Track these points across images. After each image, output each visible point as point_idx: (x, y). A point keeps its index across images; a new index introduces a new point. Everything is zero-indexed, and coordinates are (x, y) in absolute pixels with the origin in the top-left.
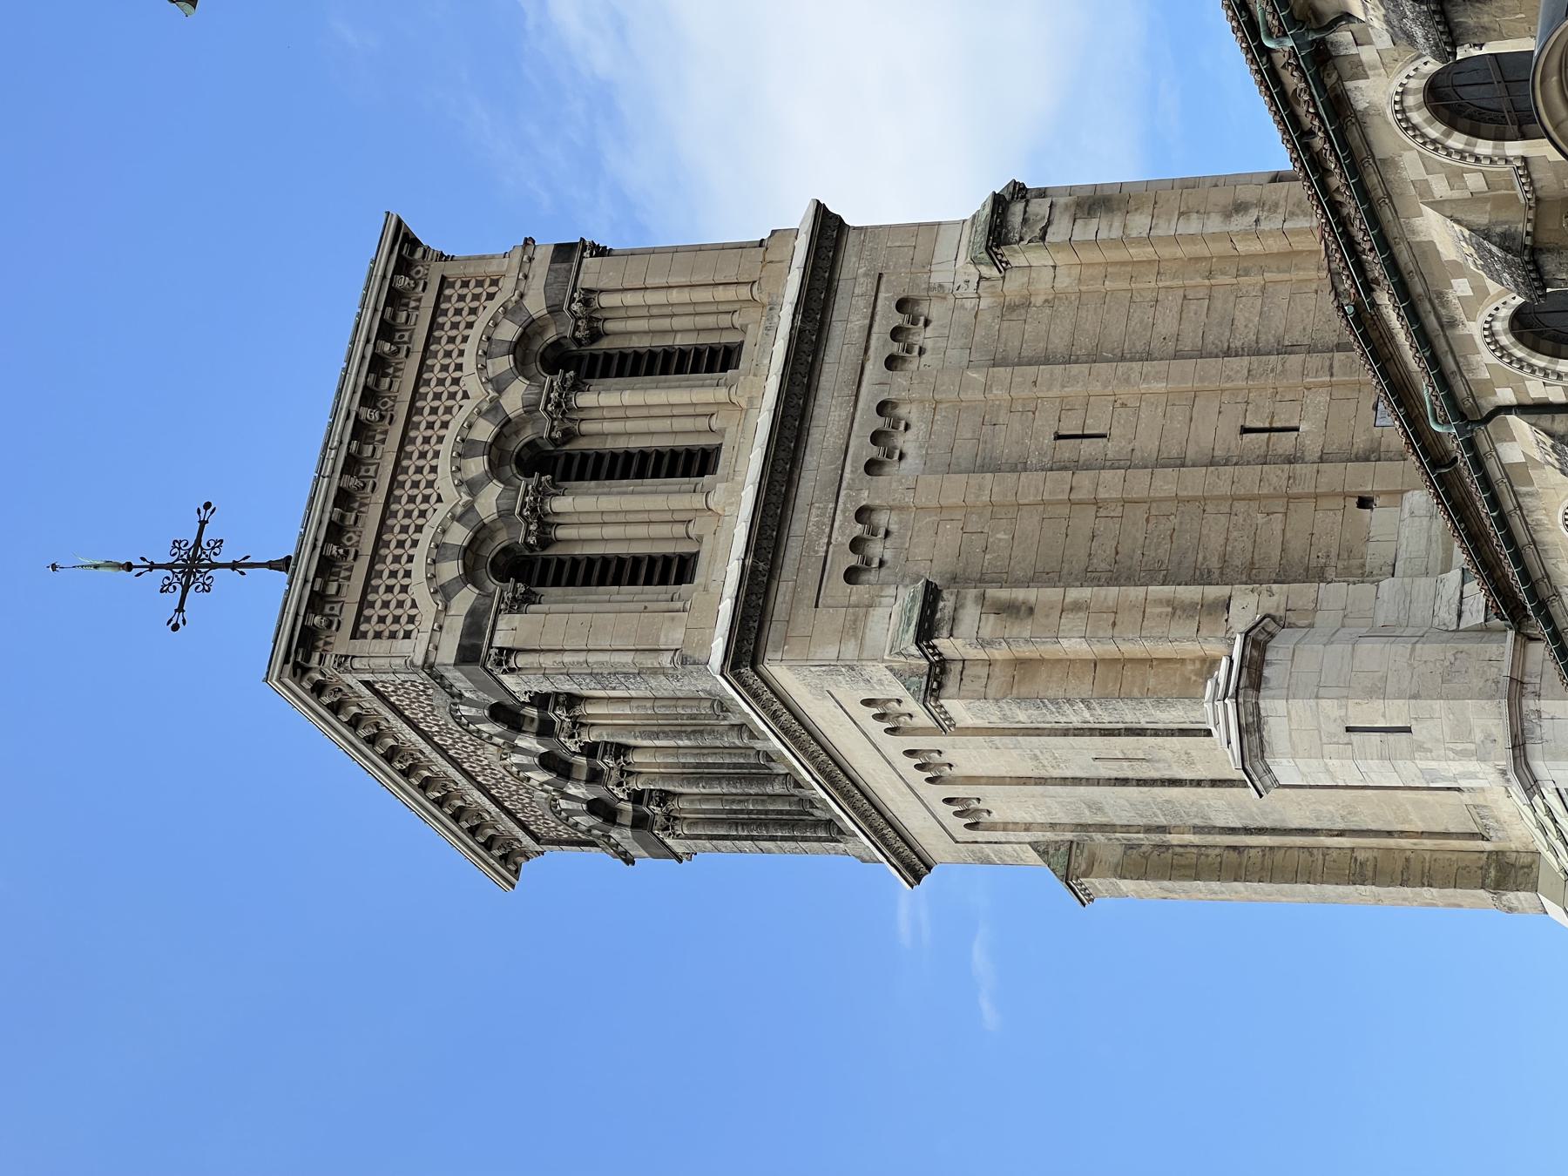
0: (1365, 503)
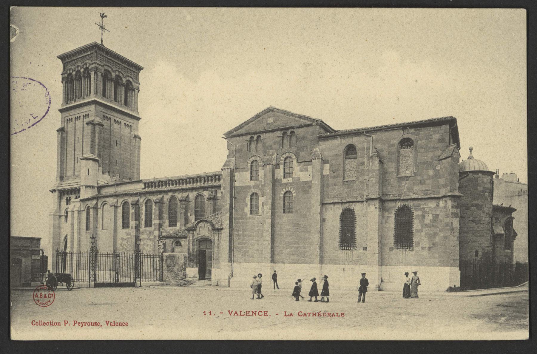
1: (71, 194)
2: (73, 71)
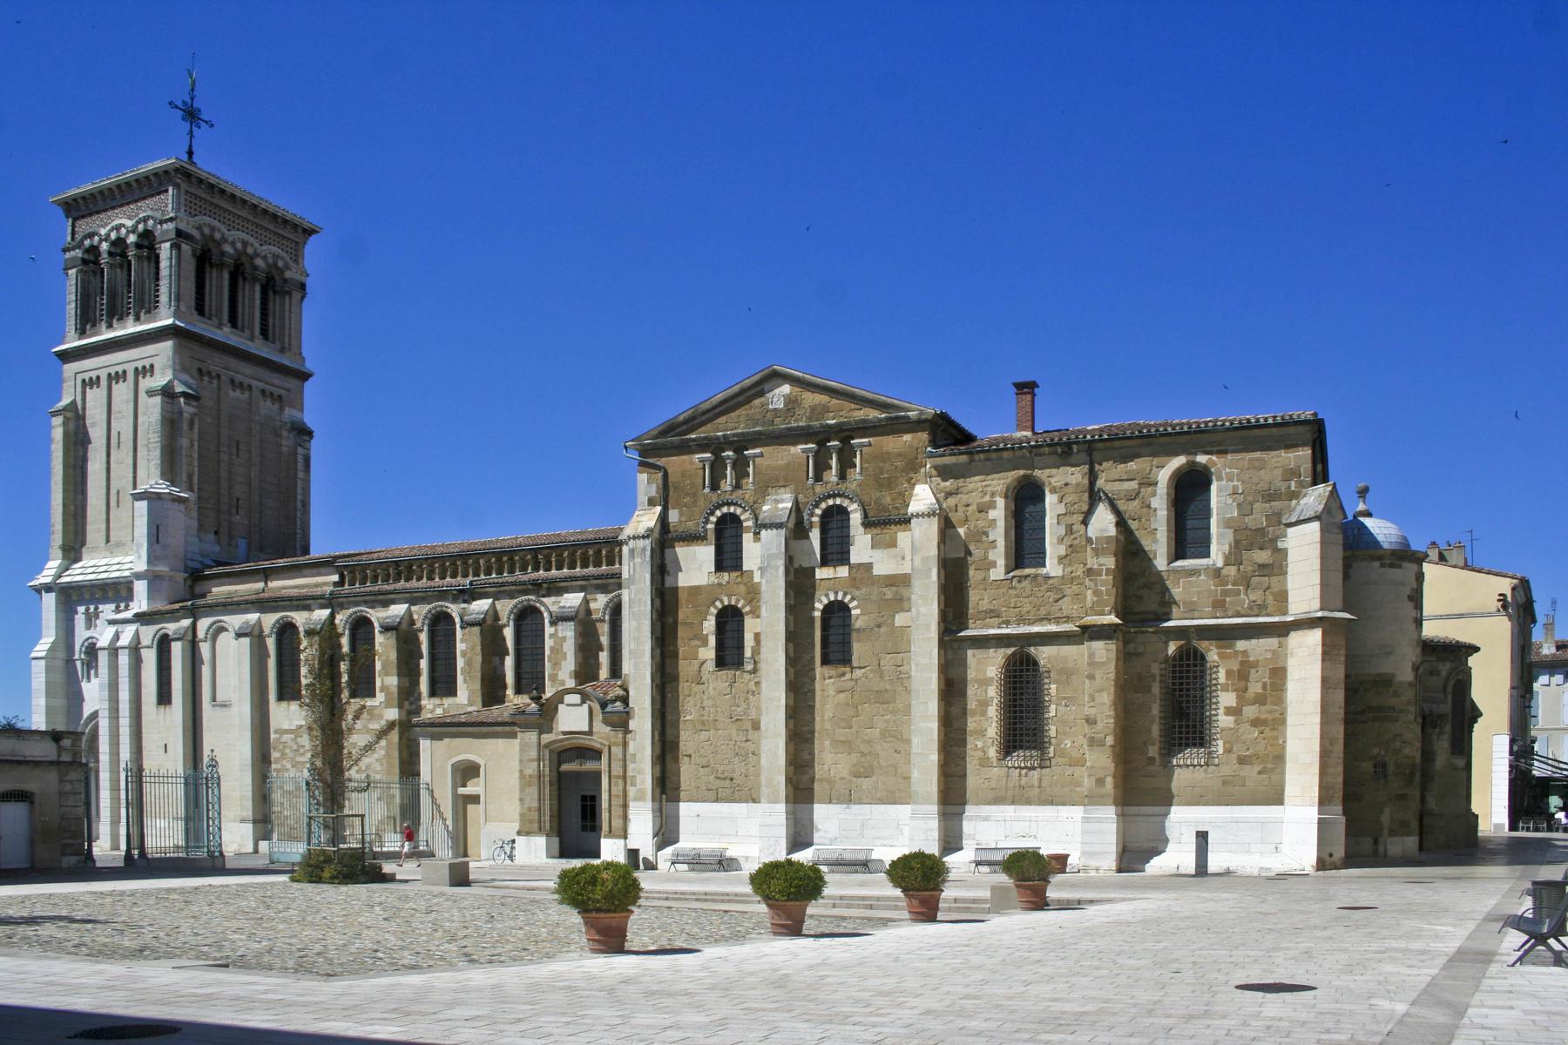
0: (216, 533)
1: (105, 600)
2: (101, 241)
